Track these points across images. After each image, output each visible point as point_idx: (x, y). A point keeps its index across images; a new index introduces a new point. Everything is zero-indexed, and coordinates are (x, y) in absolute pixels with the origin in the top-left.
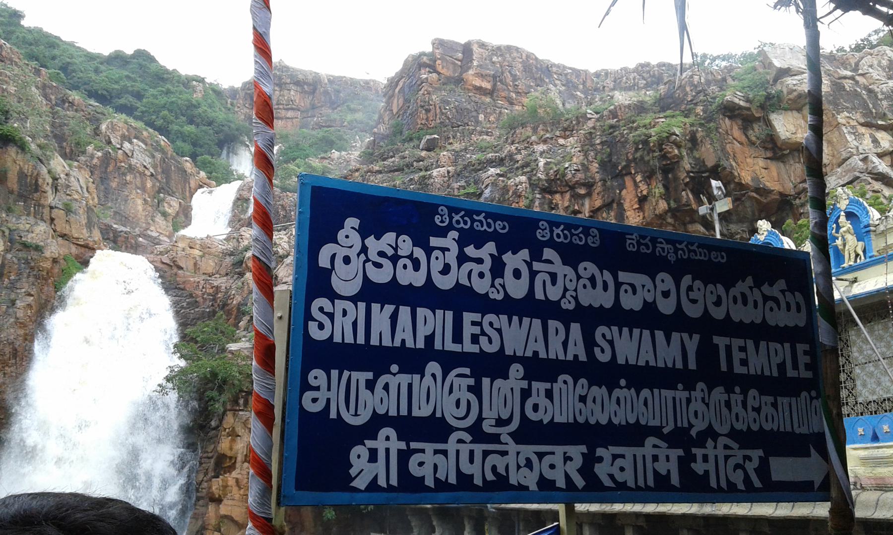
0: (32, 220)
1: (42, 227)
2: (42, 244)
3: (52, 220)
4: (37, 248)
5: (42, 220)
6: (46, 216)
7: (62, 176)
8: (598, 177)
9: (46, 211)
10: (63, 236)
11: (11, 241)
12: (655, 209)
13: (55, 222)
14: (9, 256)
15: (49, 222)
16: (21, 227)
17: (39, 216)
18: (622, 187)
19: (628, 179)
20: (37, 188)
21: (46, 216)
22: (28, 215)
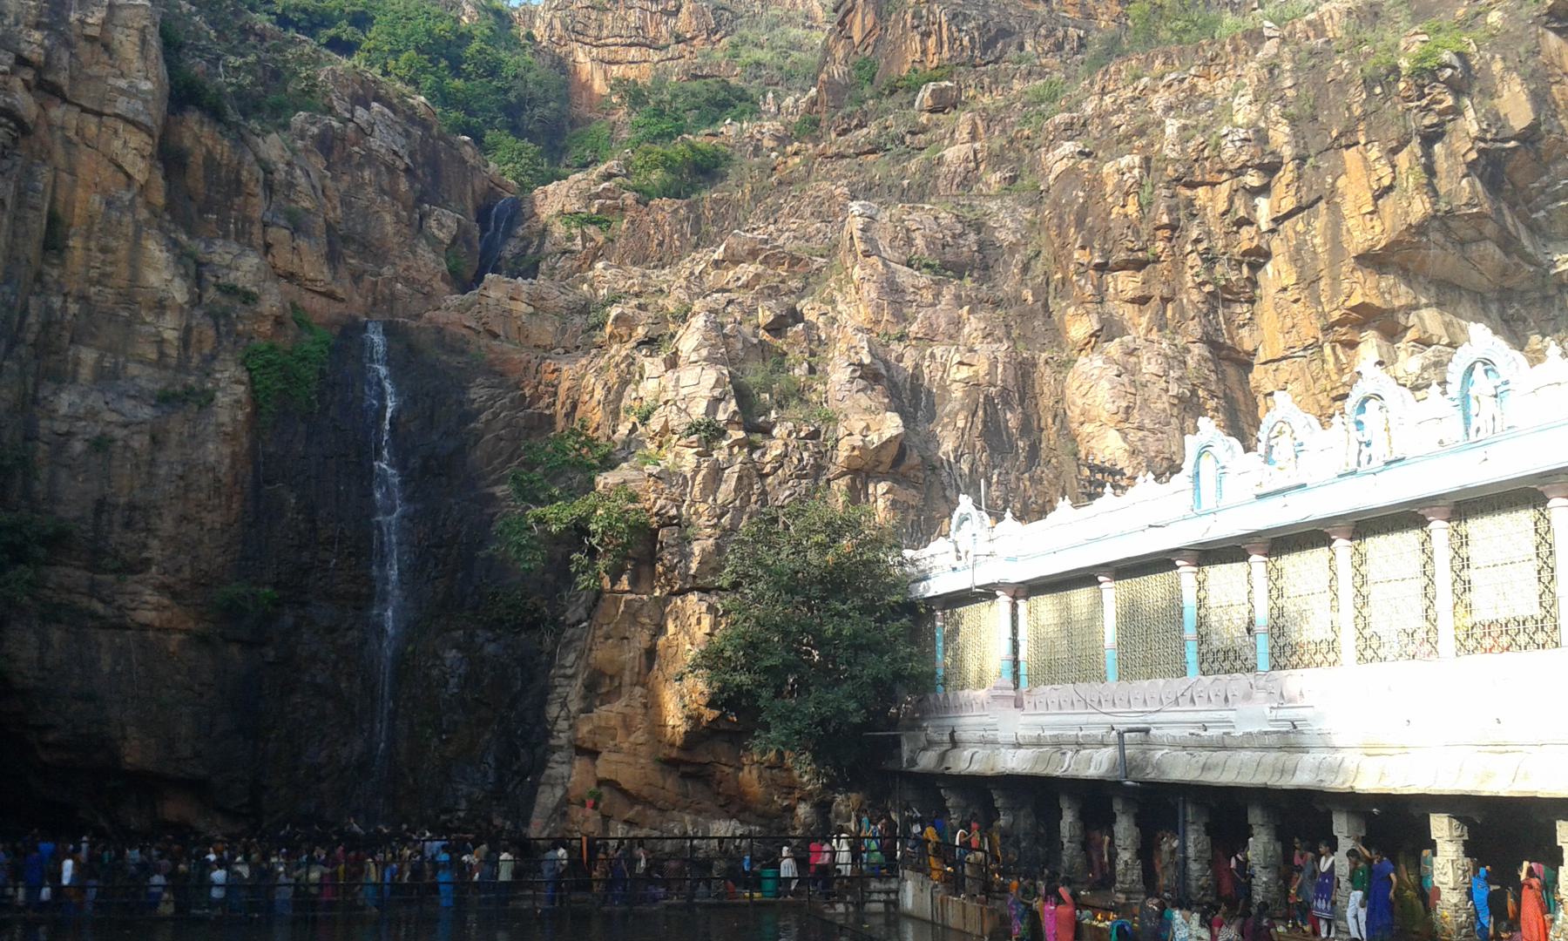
0: (235, 248)
1: (252, 261)
2: (254, 289)
3: (268, 247)
4: (249, 298)
5: (250, 246)
6: (257, 239)
7: (281, 166)
8: (1287, 152)
9: (256, 230)
10: (290, 277)
11: (199, 280)
12: (1407, 214)
13: (274, 251)
14: (198, 313)
15: (261, 251)
16: (216, 258)
17: (242, 237)
18: (1339, 171)
19: (1350, 155)
20: (237, 186)
21: (257, 239)
22: (226, 236)
